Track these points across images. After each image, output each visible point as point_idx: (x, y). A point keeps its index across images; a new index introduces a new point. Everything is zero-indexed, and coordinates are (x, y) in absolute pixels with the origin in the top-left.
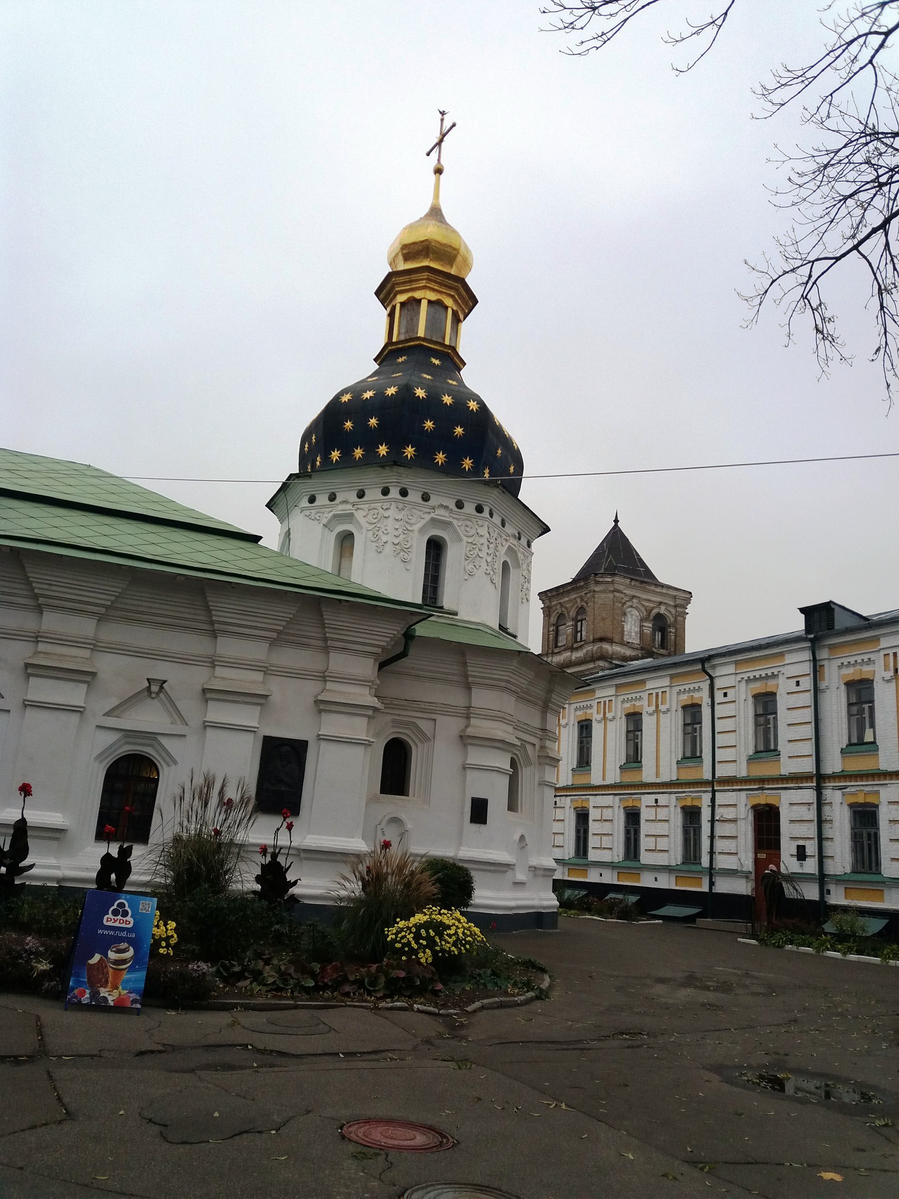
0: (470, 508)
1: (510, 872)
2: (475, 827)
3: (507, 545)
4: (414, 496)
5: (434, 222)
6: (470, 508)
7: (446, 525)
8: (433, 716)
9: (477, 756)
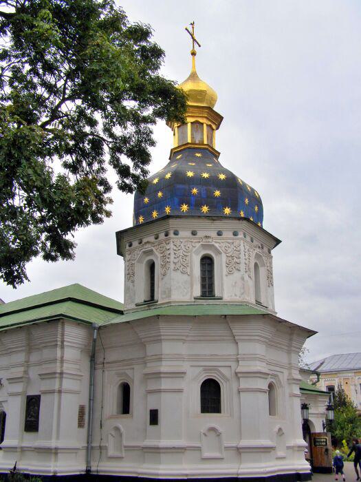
0: (162, 236)
1: (273, 452)
2: (153, 427)
3: (198, 245)
4: (135, 244)
5: (176, 86)
6: (162, 236)
7: (151, 252)
8: (132, 367)
9: (152, 386)
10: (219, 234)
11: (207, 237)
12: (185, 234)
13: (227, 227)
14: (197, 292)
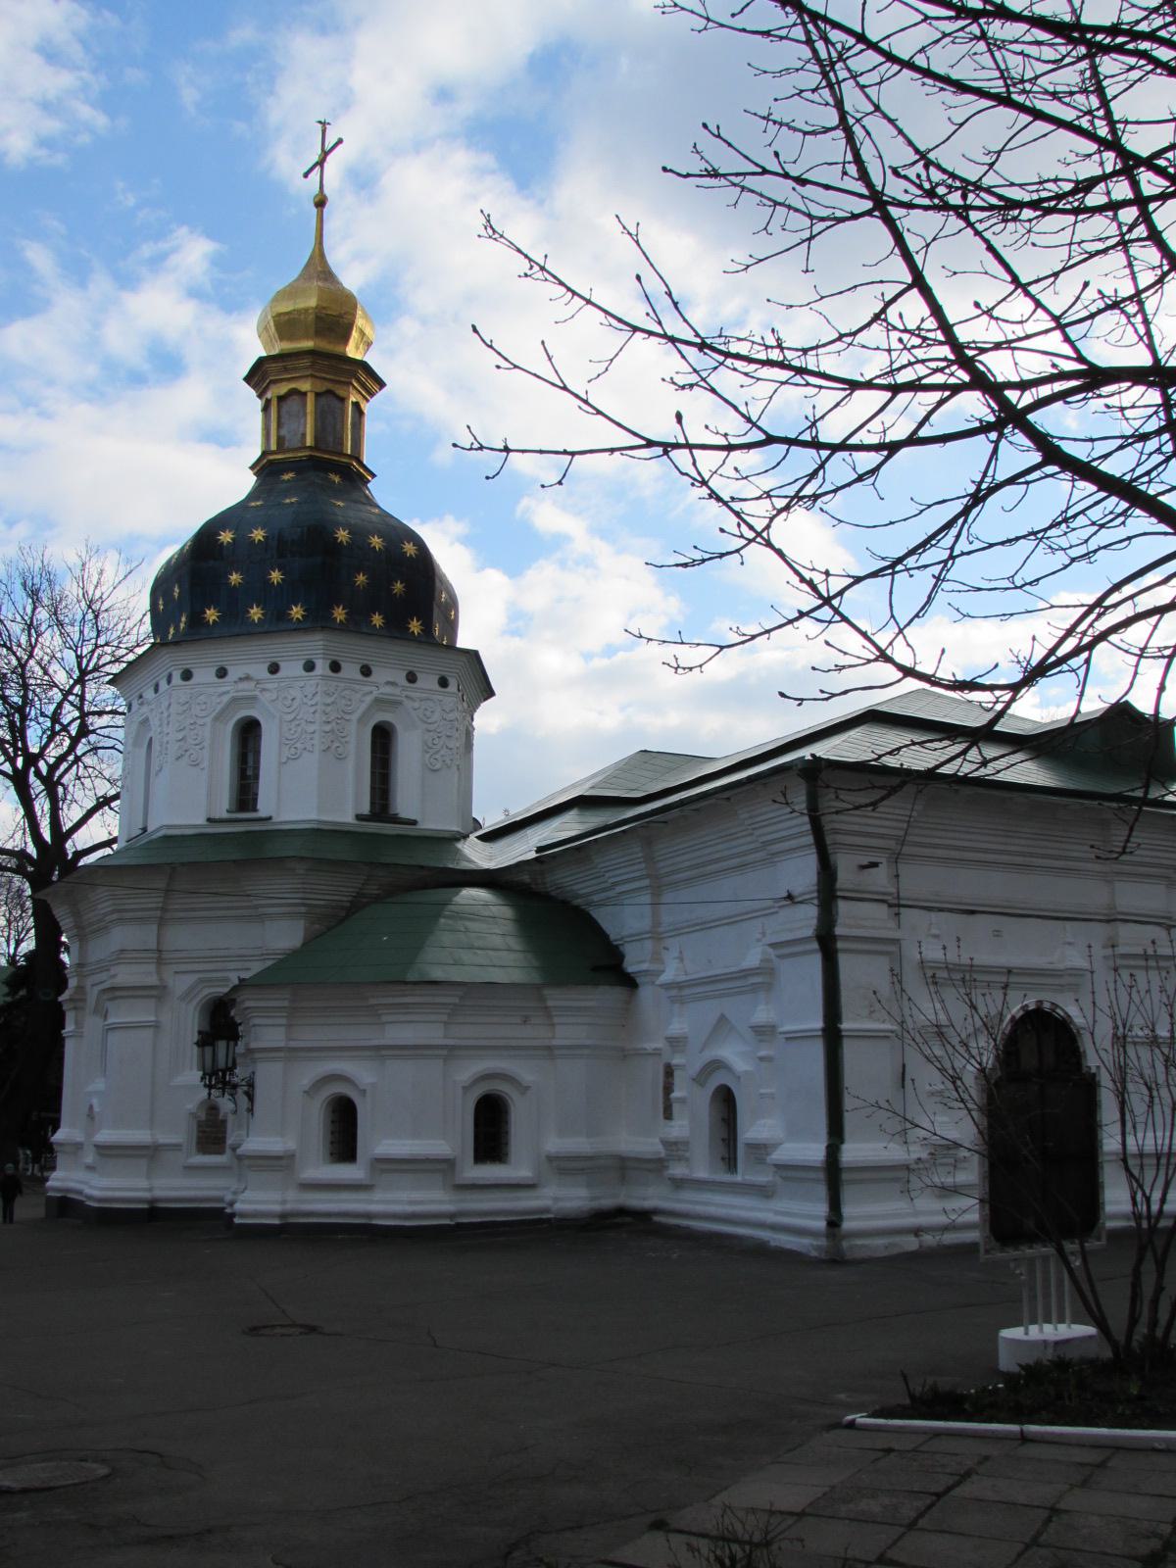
10: (274, 669)
11: (247, 678)
12: (204, 675)
13: (293, 652)
14: (222, 806)
